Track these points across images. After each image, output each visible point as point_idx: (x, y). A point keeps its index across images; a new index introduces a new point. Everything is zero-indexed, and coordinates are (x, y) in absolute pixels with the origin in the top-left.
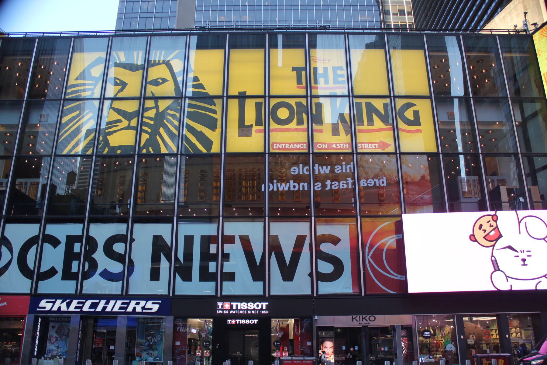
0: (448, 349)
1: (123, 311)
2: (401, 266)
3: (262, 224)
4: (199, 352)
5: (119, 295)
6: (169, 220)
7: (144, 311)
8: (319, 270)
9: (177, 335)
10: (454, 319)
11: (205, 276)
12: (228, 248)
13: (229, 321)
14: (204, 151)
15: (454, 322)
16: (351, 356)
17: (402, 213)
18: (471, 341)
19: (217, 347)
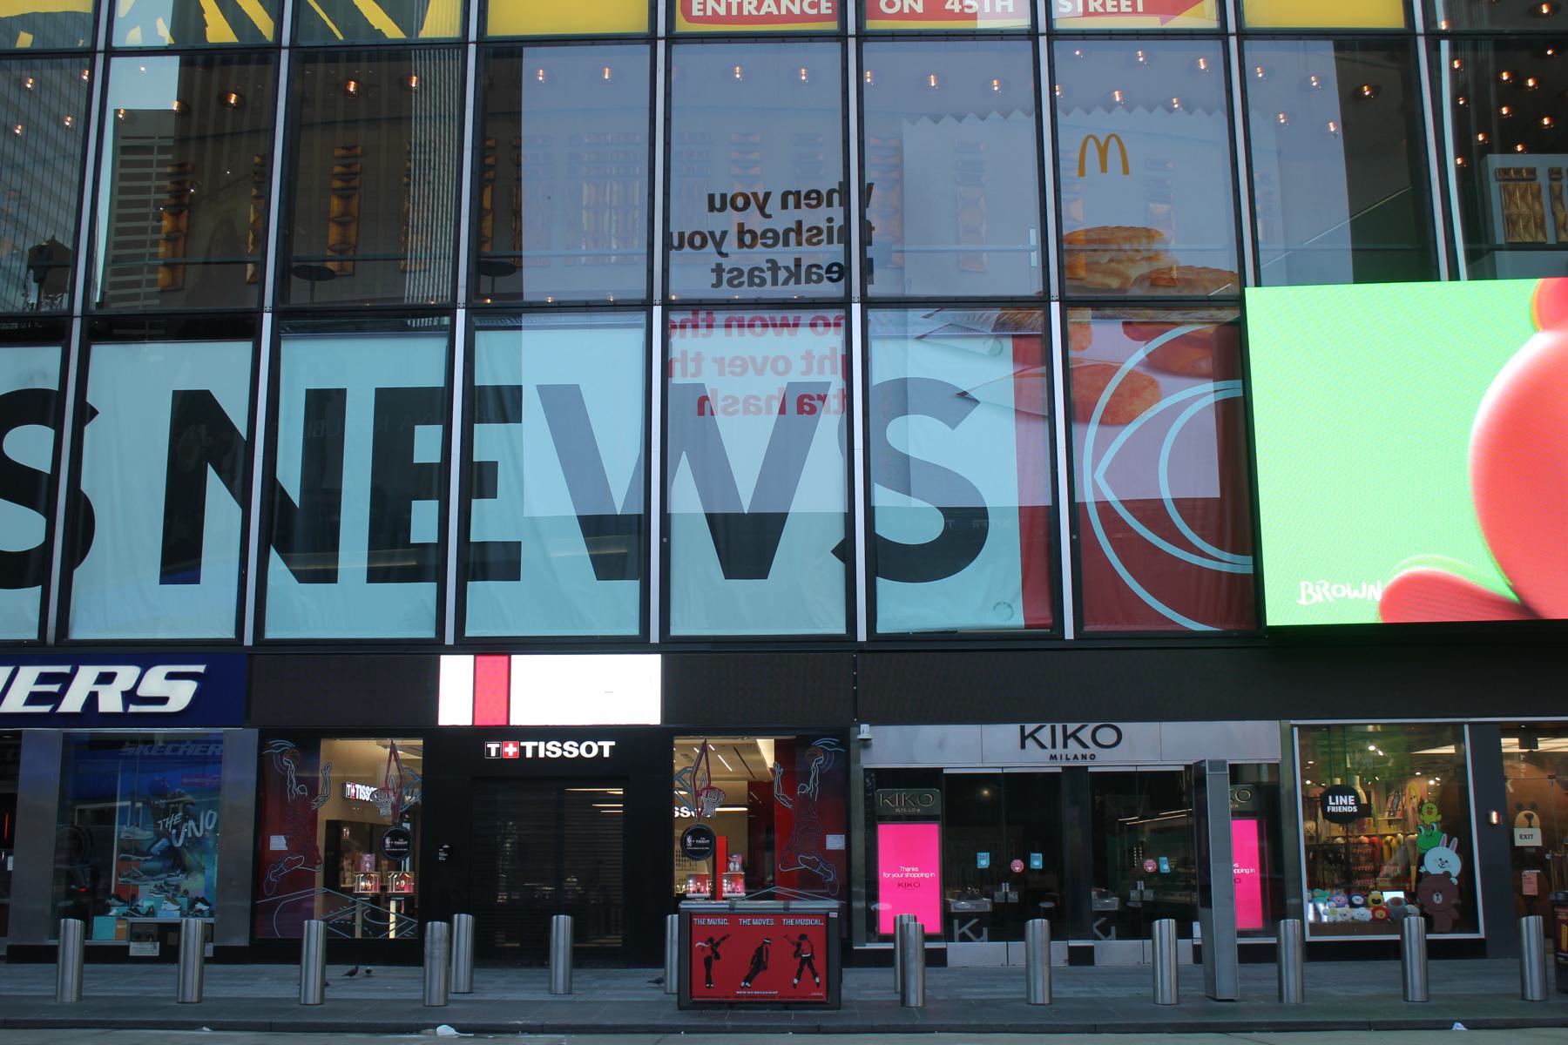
0: (1432, 865)
1: (46, 709)
2: (1235, 513)
3: (639, 335)
4: (367, 877)
5: (30, 643)
6: (240, 327)
7: (133, 709)
8: (881, 530)
9: (274, 803)
10: (1458, 740)
11: (395, 557)
12: (490, 440)
13: (493, 747)
14: (392, 31)
15: (1460, 755)
16: (1014, 897)
17: (1243, 284)
18: (1529, 836)
19: (442, 856)
